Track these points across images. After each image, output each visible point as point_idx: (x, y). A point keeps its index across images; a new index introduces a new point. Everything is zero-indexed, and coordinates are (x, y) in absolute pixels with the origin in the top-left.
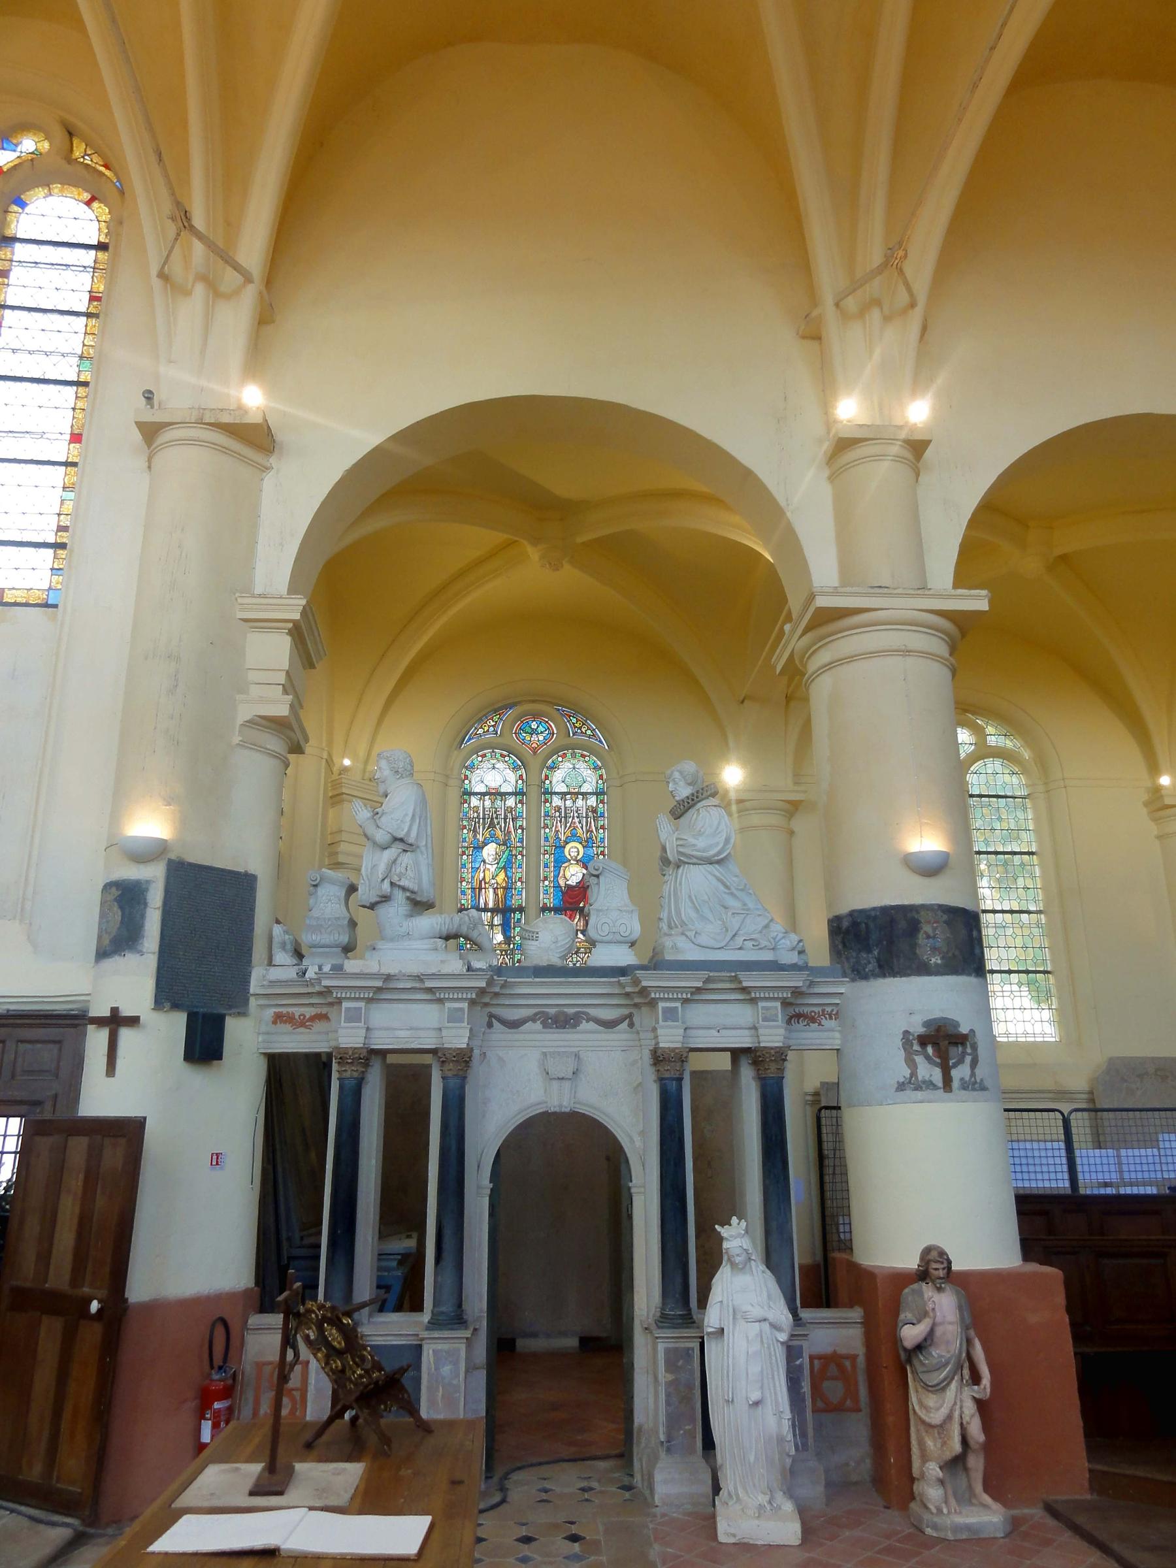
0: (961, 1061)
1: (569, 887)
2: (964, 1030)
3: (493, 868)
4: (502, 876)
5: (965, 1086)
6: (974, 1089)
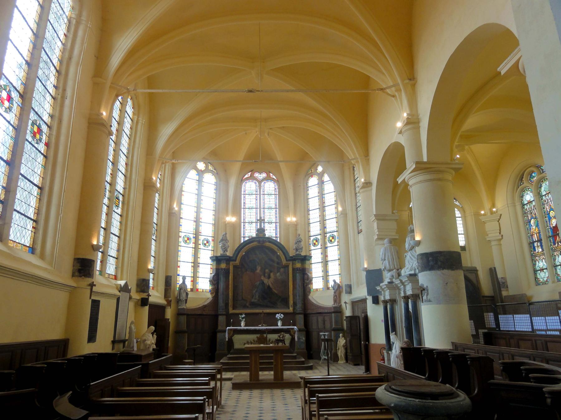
1: (553, 227)
2: (425, 286)
3: (534, 227)
4: (537, 229)
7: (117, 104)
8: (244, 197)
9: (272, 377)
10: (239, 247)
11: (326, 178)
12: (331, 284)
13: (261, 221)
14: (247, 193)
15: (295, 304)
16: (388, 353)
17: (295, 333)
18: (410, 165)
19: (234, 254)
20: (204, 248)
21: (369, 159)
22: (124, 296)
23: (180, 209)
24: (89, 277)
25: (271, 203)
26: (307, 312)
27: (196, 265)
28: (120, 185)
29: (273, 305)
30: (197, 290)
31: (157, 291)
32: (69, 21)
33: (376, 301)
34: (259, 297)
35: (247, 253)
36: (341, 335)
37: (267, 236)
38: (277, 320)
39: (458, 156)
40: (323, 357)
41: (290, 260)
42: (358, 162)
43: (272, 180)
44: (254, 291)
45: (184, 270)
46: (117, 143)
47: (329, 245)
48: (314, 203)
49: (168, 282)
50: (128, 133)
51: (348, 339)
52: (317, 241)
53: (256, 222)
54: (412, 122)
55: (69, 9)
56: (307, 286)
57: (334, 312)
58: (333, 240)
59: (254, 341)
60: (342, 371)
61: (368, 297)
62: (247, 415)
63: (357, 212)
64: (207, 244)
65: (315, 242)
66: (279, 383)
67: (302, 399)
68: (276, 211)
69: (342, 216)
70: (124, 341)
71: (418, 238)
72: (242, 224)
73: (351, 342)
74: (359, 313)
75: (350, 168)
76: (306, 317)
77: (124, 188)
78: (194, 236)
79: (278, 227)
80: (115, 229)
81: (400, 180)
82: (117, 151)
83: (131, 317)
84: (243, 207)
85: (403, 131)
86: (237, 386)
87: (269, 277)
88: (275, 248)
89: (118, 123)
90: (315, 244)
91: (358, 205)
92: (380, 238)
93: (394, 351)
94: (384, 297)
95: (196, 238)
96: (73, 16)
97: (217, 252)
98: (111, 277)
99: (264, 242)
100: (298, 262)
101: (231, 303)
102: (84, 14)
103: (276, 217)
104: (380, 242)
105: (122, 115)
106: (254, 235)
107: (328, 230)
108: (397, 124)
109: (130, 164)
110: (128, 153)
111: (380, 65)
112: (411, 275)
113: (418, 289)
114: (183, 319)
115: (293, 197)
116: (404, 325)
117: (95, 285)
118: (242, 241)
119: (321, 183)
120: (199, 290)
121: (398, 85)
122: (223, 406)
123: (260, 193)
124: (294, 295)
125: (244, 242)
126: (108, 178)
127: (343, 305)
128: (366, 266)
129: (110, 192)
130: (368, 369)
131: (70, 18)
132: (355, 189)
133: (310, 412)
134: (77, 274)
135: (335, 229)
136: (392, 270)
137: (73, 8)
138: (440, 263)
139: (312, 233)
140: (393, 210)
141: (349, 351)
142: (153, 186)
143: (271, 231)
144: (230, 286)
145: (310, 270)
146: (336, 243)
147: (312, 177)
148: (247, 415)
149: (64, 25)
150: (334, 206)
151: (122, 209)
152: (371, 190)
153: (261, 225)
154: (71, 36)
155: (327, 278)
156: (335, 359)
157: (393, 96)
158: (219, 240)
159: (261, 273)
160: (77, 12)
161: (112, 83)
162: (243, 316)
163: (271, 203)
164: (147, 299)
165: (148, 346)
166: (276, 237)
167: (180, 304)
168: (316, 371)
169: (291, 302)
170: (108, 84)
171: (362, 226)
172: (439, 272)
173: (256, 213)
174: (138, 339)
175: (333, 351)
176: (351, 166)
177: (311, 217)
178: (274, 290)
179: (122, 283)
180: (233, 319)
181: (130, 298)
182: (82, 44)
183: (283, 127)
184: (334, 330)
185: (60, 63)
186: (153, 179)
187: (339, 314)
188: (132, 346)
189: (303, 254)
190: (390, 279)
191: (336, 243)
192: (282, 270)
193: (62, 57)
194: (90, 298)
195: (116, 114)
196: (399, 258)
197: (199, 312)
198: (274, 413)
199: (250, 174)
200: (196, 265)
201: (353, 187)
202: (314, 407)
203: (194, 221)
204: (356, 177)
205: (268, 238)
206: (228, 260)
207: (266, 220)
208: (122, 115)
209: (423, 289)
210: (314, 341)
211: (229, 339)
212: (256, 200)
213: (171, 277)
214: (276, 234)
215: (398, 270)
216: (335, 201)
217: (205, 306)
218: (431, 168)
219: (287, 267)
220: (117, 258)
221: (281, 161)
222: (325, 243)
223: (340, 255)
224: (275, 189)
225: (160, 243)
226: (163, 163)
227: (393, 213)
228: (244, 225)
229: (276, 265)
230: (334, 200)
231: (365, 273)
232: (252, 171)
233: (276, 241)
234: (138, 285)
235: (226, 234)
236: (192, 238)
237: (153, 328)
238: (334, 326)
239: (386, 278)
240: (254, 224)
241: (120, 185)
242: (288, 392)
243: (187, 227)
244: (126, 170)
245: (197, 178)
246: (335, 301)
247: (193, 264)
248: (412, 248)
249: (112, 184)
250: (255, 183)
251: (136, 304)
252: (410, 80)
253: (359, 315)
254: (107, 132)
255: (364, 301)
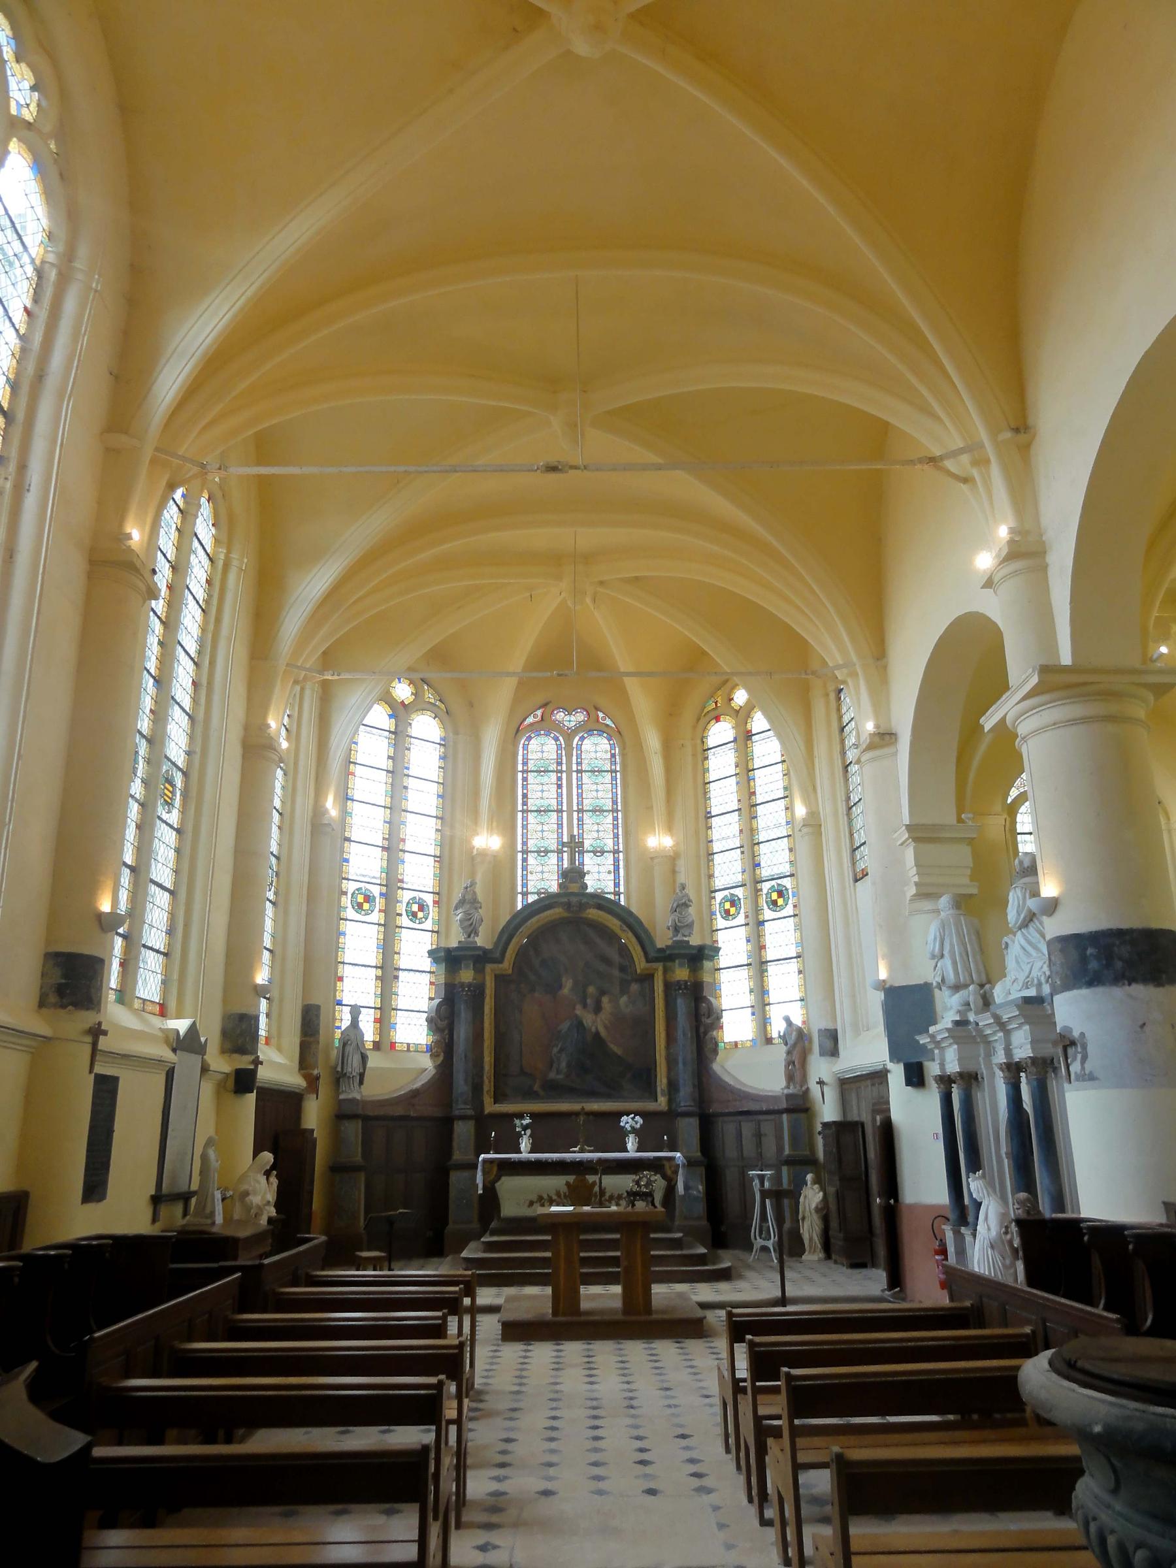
0: (1075, 1059)
2: (1076, 1034)
5: (1077, 1079)
6: (1084, 1080)
7: (171, 514)
8: (525, 779)
9: (618, 1304)
10: (509, 922)
11: (759, 722)
12: (777, 1028)
13: (575, 846)
14: (531, 766)
15: (673, 1086)
16: (957, 1233)
17: (676, 1172)
18: (1021, 673)
19: (496, 944)
20: (411, 925)
21: (885, 668)
22: (186, 1065)
23: (345, 813)
24: (88, 1009)
25: (600, 794)
26: (709, 1110)
27: (388, 973)
28: (177, 746)
29: (611, 1090)
30: (393, 1045)
31: (279, 1049)
32: (40, 273)
33: (915, 1077)
34: (569, 1065)
35: (536, 939)
36: (809, 1177)
37: (590, 890)
38: (623, 1134)
39: (1164, 650)
40: (759, 1242)
41: (657, 960)
42: (854, 675)
43: (602, 730)
44: (555, 1050)
45: (357, 988)
46: (170, 624)
47: (768, 914)
48: (723, 796)
49: (311, 1021)
50: (201, 595)
51: (831, 1190)
52: (733, 904)
53: (560, 852)
54: (1026, 553)
55: (40, 237)
56: (706, 1033)
57: (788, 1111)
58: (780, 901)
59: (558, 1194)
60: (825, 1284)
61: (890, 1066)
62: (555, 1423)
63: (850, 821)
64: (420, 915)
65: (727, 906)
66: (639, 1323)
67: (721, 1377)
68: (615, 819)
69: (805, 830)
70: (185, 1197)
71: (1049, 888)
72: (520, 855)
73: (839, 1197)
74: (862, 1113)
75: (827, 695)
76: (707, 1123)
77: (188, 753)
78: (384, 890)
79: (621, 863)
80: (162, 870)
81: (989, 722)
82: (168, 645)
83: (206, 1128)
84: (520, 808)
85: (996, 579)
86: (518, 1331)
87: (598, 1009)
88: (614, 923)
89: (174, 568)
90: (727, 912)
91: (854, 798)
92: (926, 893)
93: (981, 1227)
94: (942, 1065)
95: (390, 896)
96: (51, 258)
97: (447, 936)
98: (149, 1008)
99: (582, 907)
100: (681, 965)
101: (488, 1086)
102: (83, 251)
103: (616, 836)
104: (927, 905)
105: (182, 541)
106: (554, 888)
107: (765, 872)
108: (980, 557)
109: (204, 682)
110: (199, 653)
111: (925, 392)
112: (1027, 1000)
113: (1055, 1043)
114: (353, 1130)
115: (667, 779)
116: (1004, 1150)
117: (105, 1033)
118: (519, 906)
119: (745, 738)
120: (398, 1047)
121: (982, 446)
122: (480, 1392)
123: (567, 768)
124: (671, 1062)
125: (526, 907)
126: (144, 725)
127: (815, 1090)
128: (883, 974)
129: (148, 761)
130: (896, 1280)
131: (43, 262)
132: (843, 753)
133: (758, 1419)
134: (53, 998)
135: (786, 869)
136: (966, 986)
137: (50, 236)
138: (1119, 965)
139: (719, 883)
140: (960, 809)
141: (834, 1224)
142: (269, 745)
143: (602, 876)
144: (487, 1035)
145: (715, 987)
146: (789, 910)
147: (717, 719)
148: (555, 1423)
149: (26, 284)
150: (782, 804)
151: (183, 812)
152: (895, 754)
153: (572, 860)
154: (43, 315)
155: (764, 1012)
156: (791, 1247)
157: (965, 480)
158: (455, 901)
159: (574, 996)
160: (61, 248)
161: (157, 449)
162: (527, 1121)
163: (600, 794)
164: (253, 1073)
165: (253, 1212)
166: (617, 894)
167: (343, 1087)
168: (741, 1284)
169: (662, 1082)
170: (148, 452)
171: (868, 859)
172: (1118, 992)
173: (560, 826)
174: (226, 1189)
175: (787, 1225)
176: (831, 688)
177: (715, 834)
178: (612, 1046)
179: (181, 1025)
180: (494, 1131)
181: (205, 1069)
182: (76, 335)
183: (637, 578)
184: (790, 1162)
185: (12, 388)
186: (269, 726)
187: (803, 1116)
188: (208, 1211)
189: (695, 941)
190: (959, 1012)
191: (789, 910)
192: (635, 987)
193: (19, 373)
194: (91, 1072)
195: (167, 541)
196: (982, 950)
197: (399, 1111)
198: (633, 1416)
199: (539, 713)
200: (388, 973)
201: (838, 748)
202: (775, 1407)
203: (384, 849)
204: (846, 719)
205: (594, 896)
206: (481, 958)
207: (587, 844)
208: (182, 541)
209: (1068, 1043)
210: (732, 1195)
211: (484, 1188)
212: (559, 786)
213: (318, 1007)
214: (617, 885)
215: (982, 986)
216: (785, 789)
217: (415, 1094)
218: (1085, 684)
219: (648, 978)
220: (165, 955)
221: (629, 674)
222: (757, 910)
223: (801, 943)
224: (613, 756)
225: (286, 912)
226: (296, 682)
227: (960, 820)
228: (525, 860)
229: (616, 973)
230: (781, 785)
231: (881, 996)
232: (544, 705)
233: (617, 904)
234: (225, 1034)
235: (473, 884)
236: (377, 895)
237: (268, 1157)
238: (787, 1152)
239: (946, 1009)
240: (553, 858)
241: (177, 746)
242: (666, 1349)
243: (363, 864)
244: (195, 700)
245: (387, 723)
246: (790, 1078)
247: (379, 972)
248: (1031, 917)
249: (156, 740)
250: (556, 739)
251: (220, 1087)
252: (1017, 430)
253: (865, 1117)
254: (144, 589)
255: (879, 1077)
